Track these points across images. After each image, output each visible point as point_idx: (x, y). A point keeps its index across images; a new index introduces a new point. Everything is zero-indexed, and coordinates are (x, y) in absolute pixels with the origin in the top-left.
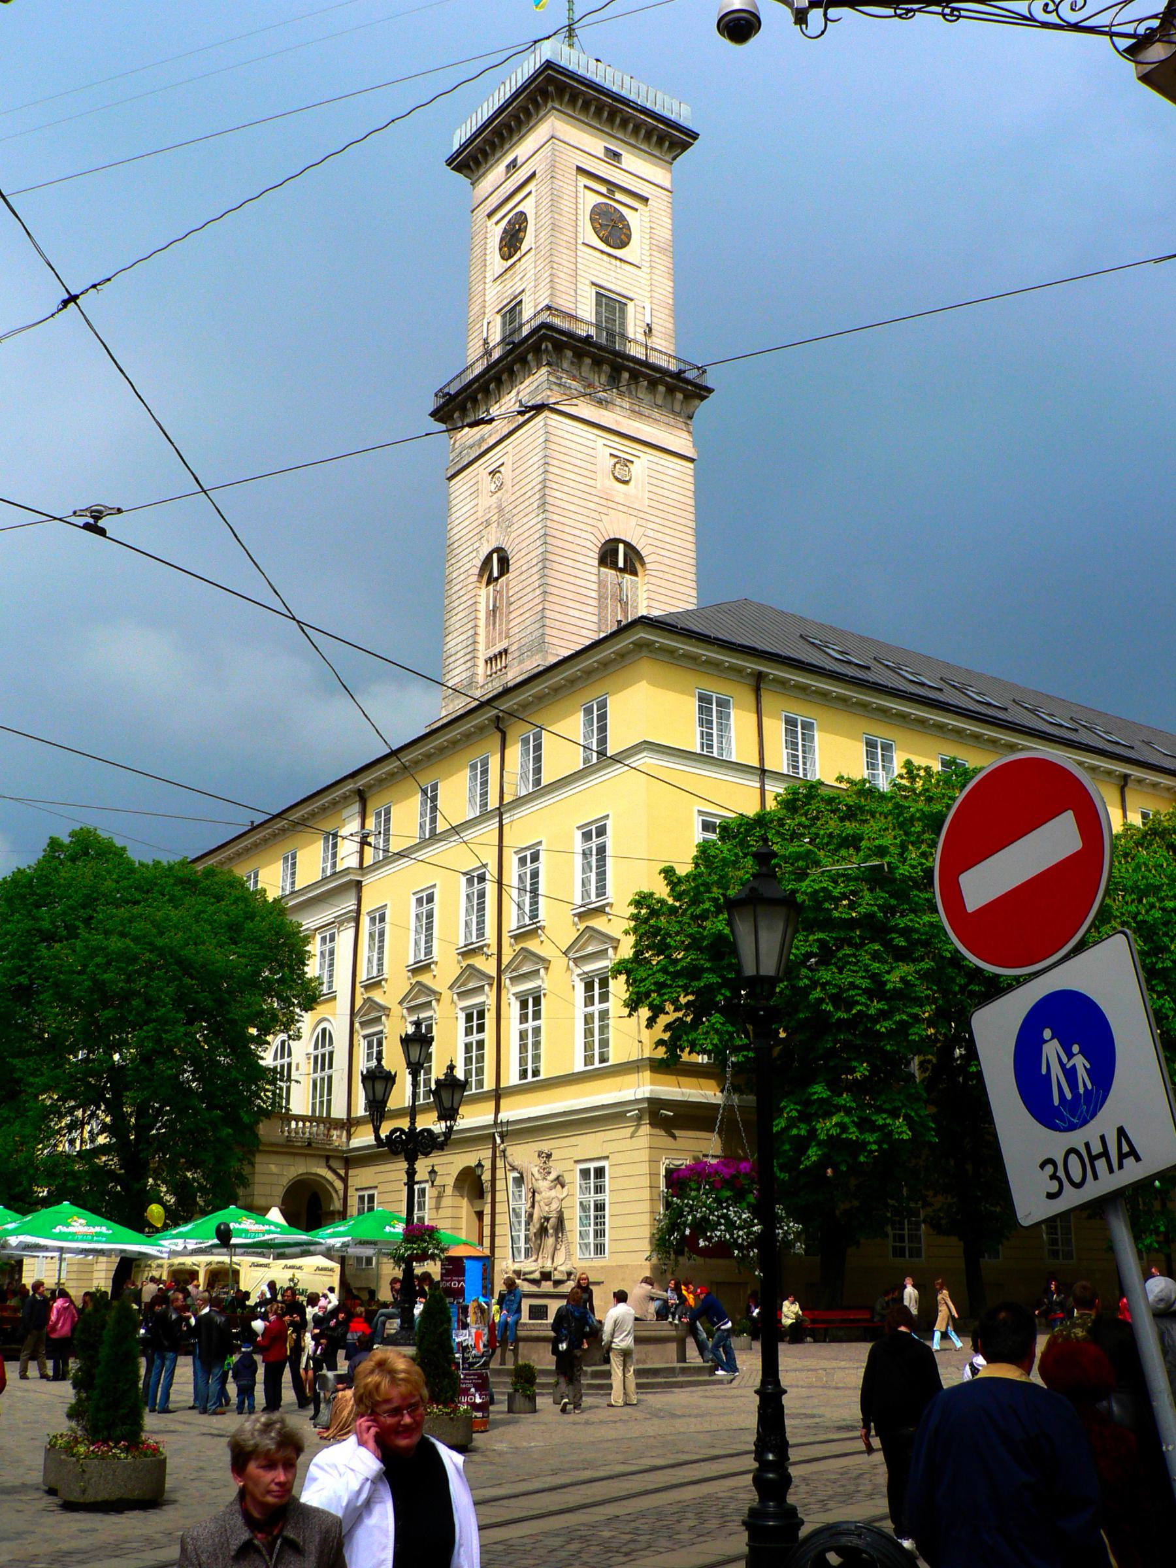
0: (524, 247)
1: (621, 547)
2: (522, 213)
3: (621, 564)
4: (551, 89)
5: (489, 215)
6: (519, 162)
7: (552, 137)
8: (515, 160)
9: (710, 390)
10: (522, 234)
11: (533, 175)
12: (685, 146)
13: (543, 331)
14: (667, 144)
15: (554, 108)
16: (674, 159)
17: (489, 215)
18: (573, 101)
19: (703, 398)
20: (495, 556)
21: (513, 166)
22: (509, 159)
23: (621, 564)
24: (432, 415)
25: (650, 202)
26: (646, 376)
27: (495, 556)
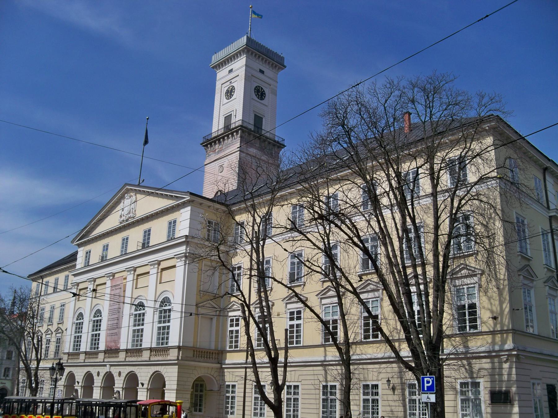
4: (246, 51)
8: (232, 69)
10: (233, 93)
11: (238, 75)
12: (283, 69)
14: (277, 68)
17: (222, 84)
21: (231, 71)
22: (230, 68)
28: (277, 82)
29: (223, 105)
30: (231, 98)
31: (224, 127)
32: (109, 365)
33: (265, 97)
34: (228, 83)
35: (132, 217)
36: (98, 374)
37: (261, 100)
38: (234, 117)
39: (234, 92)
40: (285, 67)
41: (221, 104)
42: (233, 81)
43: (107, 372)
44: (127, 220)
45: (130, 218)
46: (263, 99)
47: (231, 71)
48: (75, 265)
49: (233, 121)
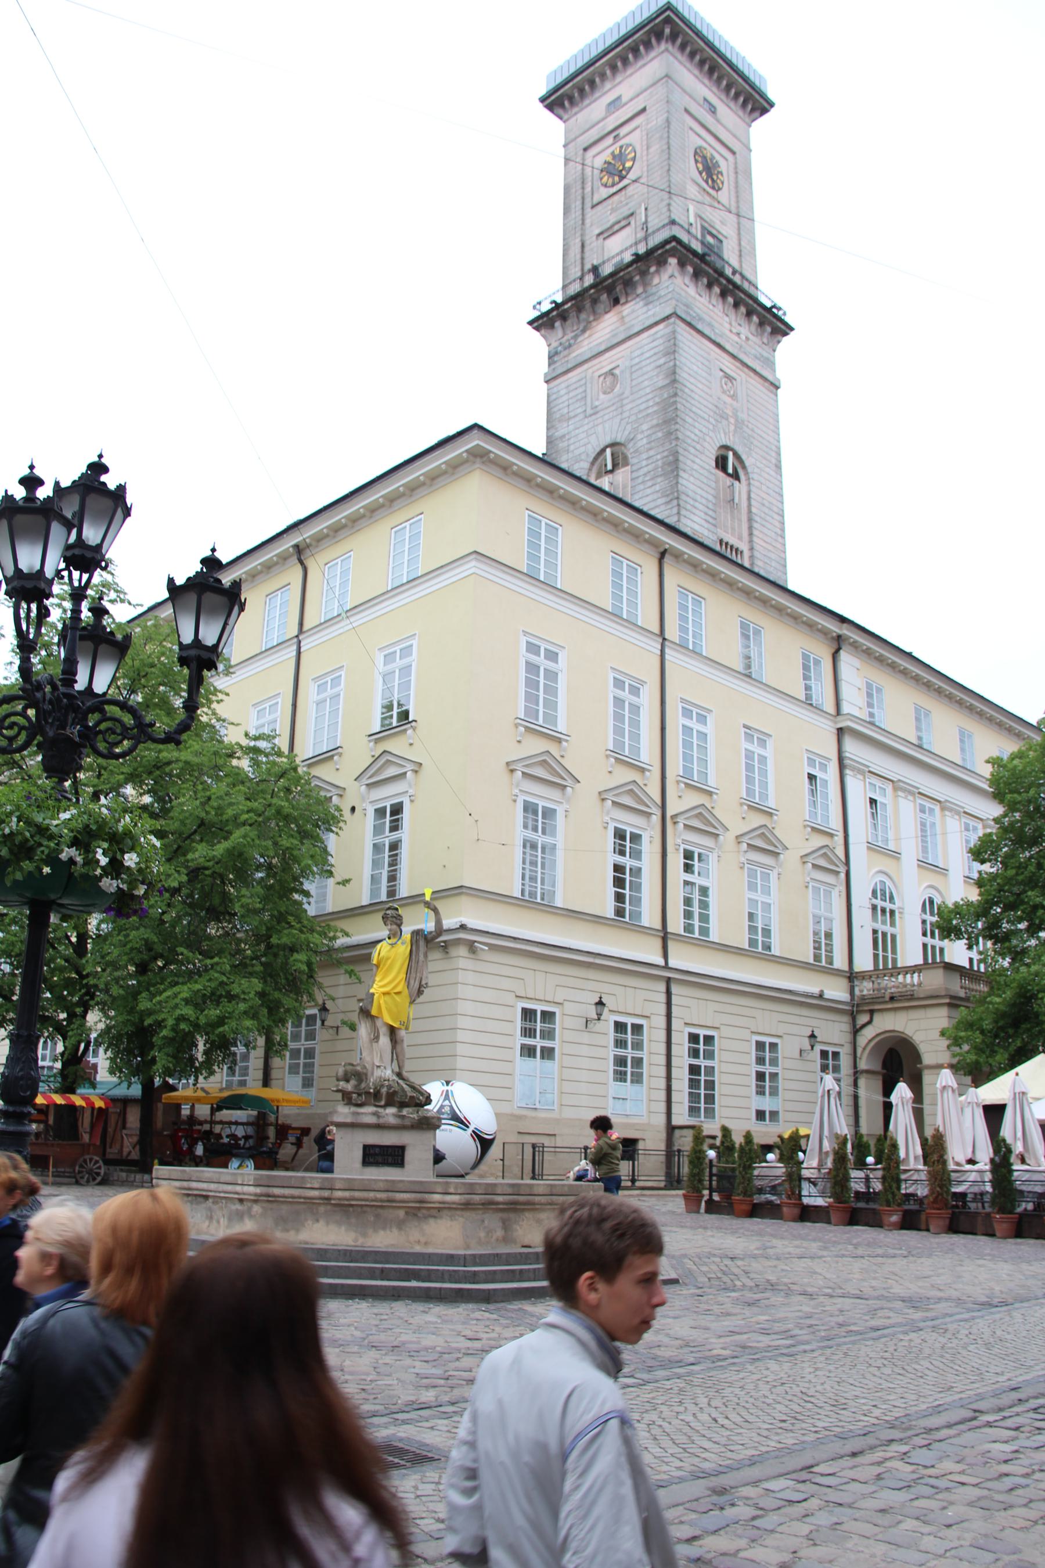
0: (632, 176)
1: (730, 455)
3: (730, 471)
4: (667, 31)
5: (585, 150)
6: (624, 100)
7: (667, 76)
8: (619, 98)
9: (792, 329)
10: (628, 165)
11: (644, 110)
12: (764, 111)
13: (674, 244)
14: (750, 107)
15: (667, 50)
16: (754, 120)
17: (585, 150)
18: (682, 48)
19: (785, 334)
20: (608, 451)
21: (615, 104)
23: (730, 471)
24: (530, 323)
25: (738, 156)
26: (746, 305)
27: (608, 451)
28: (750, 151)
33: (722, 183)
34: (610, 140)
37: (713, 188)
39: (634, 159)
40: (772, 105)
42: (623, 131)
46: (719, 189)
47: (615, 104)
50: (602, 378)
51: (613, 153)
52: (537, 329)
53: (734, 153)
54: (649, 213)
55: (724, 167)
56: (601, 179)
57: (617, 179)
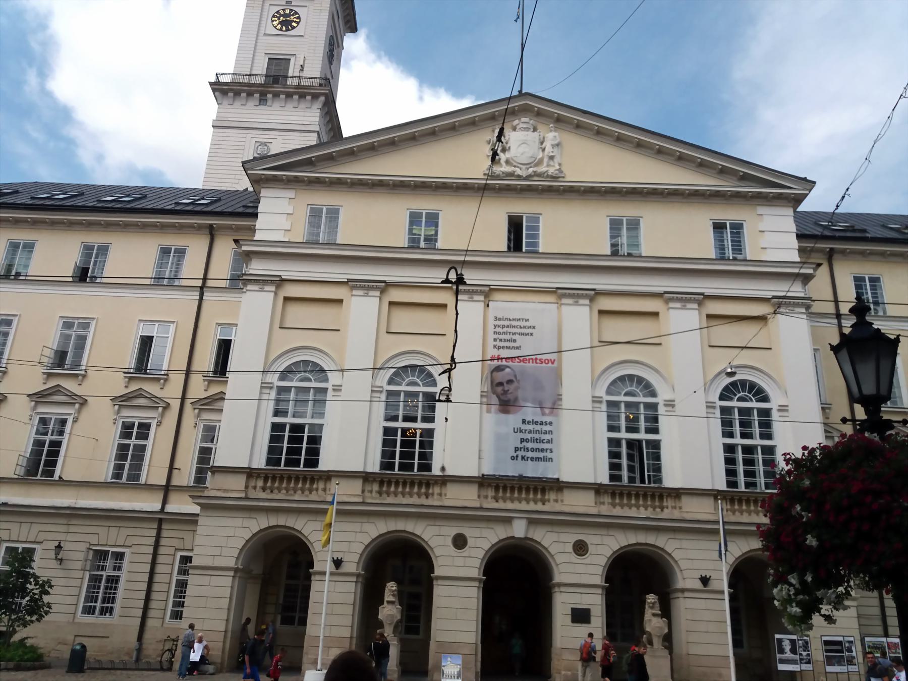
2: (296, 13)
14: (348, 25)
24: (211, 84)
28: (343, 49)
29: (265, 34)
30: (288, 30)
31: (267, 76)
32: (527, 518)
35: (552, 177)
36: (460, 542)
38: (298, 68)
39: (298, 23)
41: (262, 32)
43: (513, 537)
44: (528, 178)
45: (536, 174)
48: (252, 230)
49: (293, 70)
50: (259, 144)
51: (284, 10)
52: (214, 90)
53: (338, 47)
54: (306, 62)
55: (335, 53)
56: (273, 21)
57: (284, 28)
